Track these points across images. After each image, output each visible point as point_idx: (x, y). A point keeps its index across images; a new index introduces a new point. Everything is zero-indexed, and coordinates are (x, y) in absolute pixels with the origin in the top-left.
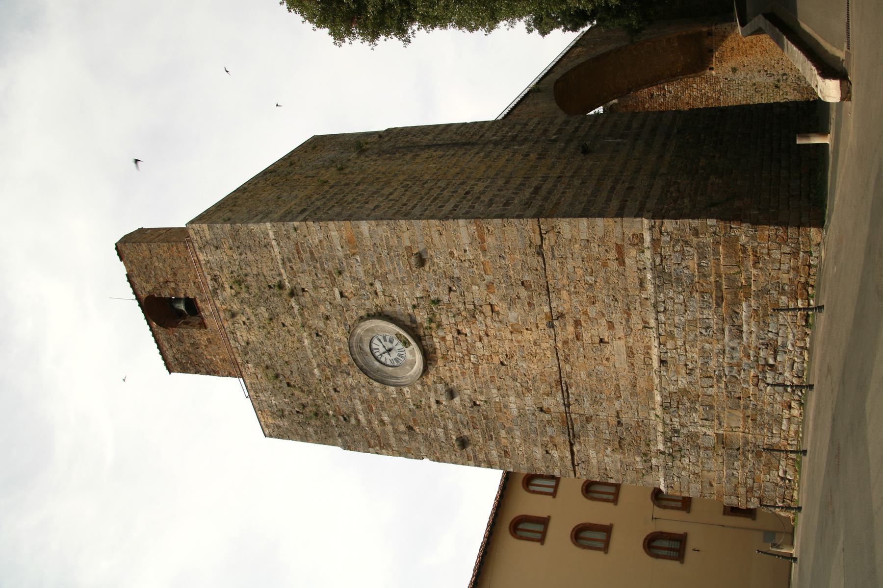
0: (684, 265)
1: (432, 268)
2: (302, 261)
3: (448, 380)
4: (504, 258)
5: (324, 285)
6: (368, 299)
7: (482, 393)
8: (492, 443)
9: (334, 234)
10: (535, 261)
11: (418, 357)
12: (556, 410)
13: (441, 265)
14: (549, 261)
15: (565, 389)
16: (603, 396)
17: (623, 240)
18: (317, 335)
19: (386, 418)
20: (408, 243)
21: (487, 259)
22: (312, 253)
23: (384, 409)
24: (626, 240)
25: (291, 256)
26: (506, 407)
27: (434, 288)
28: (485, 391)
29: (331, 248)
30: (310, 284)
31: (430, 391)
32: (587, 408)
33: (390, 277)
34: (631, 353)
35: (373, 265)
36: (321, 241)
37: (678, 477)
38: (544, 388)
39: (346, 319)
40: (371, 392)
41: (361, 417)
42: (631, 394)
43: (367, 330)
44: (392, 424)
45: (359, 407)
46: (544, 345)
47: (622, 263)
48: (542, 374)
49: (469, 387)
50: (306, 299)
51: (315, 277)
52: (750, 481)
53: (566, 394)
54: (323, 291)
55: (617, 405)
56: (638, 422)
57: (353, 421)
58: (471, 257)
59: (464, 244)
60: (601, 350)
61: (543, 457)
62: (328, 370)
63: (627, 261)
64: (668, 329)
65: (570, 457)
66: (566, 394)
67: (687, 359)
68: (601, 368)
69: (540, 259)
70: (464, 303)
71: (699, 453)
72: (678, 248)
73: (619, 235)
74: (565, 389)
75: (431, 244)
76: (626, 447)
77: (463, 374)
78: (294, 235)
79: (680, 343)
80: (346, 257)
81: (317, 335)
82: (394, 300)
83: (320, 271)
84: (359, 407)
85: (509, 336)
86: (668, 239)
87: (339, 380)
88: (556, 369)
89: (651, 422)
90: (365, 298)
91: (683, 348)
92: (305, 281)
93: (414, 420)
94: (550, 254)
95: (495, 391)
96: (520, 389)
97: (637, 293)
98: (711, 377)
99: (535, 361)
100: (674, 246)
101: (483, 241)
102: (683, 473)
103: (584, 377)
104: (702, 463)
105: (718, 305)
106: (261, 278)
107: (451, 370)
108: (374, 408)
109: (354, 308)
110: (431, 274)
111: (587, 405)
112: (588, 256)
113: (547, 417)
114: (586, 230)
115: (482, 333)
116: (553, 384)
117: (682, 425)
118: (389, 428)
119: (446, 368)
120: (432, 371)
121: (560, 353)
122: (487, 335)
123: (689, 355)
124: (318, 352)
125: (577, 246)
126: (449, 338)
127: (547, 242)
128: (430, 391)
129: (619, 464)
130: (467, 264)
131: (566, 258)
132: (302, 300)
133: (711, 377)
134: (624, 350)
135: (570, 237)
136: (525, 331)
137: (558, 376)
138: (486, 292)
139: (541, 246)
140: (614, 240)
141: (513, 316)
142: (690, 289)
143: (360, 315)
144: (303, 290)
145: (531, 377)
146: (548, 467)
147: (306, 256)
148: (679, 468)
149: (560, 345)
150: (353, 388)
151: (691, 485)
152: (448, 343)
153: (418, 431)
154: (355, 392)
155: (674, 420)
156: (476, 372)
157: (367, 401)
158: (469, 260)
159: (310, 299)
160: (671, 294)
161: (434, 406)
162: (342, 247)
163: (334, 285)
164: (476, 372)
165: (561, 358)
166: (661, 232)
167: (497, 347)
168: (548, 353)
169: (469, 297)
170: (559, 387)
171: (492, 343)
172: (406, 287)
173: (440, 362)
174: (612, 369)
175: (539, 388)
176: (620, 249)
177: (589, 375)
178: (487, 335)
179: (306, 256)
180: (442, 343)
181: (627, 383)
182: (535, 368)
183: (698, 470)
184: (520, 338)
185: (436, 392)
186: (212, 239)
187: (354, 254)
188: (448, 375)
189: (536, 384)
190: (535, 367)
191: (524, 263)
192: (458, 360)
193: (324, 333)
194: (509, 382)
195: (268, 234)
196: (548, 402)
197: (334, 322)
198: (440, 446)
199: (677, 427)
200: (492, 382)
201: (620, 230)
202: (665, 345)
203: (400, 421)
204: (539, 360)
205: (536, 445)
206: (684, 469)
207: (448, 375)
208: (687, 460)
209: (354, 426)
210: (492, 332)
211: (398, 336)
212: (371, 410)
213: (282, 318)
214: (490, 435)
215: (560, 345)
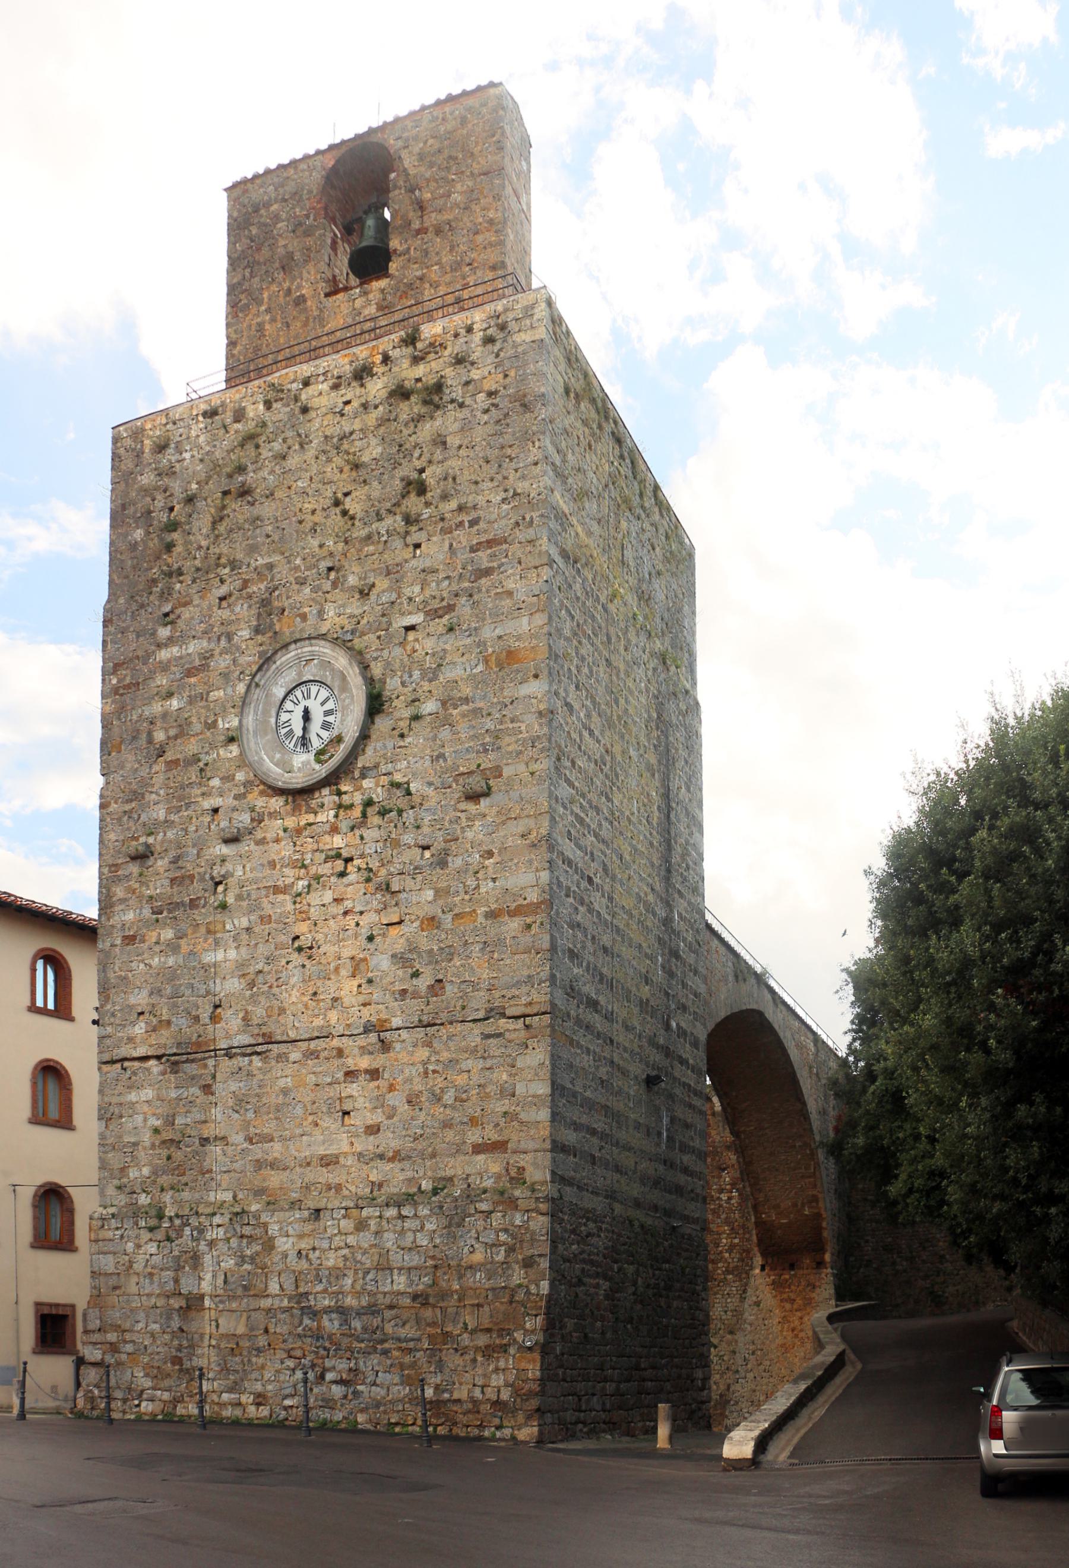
0: (476, 1246)
1: (463, 815)
2: (473, 550)
3: (259, 834)
4: (482, 950)
5: (428, 593)
6: (403, 684)
7: (239, 898)
8: (147, 912)
9: (524, 624)
10: (478, 1003)
11: (298, 780)
12: (220, 1034)
13: (469, 834)
14: (478, 1029)
15: (259, 1049)
16: (250, 1115)
17: (515, 1152)
18: (330, 569)
19: (175, 703)
20: (507, 772)
21: (481, 919)
22: (488, 572)
23: (191, 701)
24: (516, 1157)
25: (482, 525)
26: (217, 943)
27: (428, 818)
28: (245, 904)
29: (497, 617)
30: (428, 563)
31: (236, 797)
32: (227, 1088)
33: (445, 733)
34: (329, 1162)
35: (466, 700)
36: (510, 593)
37: (122, 1237)
38: (258, 1012)
39: (363, 634)
40: (225, 676)
41: (175, 651)
42: (258, 1161)
43: (344, 678)
44: (165, 715)
45: (193, 647)
46: (333, 1016)
47: (478, 1149)
48: (282, 1011)
49: (249, 875)
50: (399, 552)
51: (442, 575)
52: (129, 1348)
53: (250, 1051)
54: (417, 589)
55: (238, 1138)
56: (210, 1171)
57: (164, 632)
58: (483, 890)
59: (506, 878)
60: (329, 1113)
61: (131, 1007)
62: (262, 586)
63: (481, 1158)
64: (372, 1222)
65: (136, 1054)
66: (250, 1051)
67: (324, 1251)
68: (299, 1111)
69: (481, 1015)
70: (403, 873)
71: (168, 1269)
72: (503, 1237)
73: (523, 1145)
74: (259, 1049)
75: (506, 817)
76: (165, 1153)
77: (272, 864)
78: (521, 535)
79: (351, 1240)
80: (481, 644)
81: (330, 569)
82: (402, 736)
83: (455, 587)
84: (193, 647)
85: (346, 953)
86: (518, 1222)
87: (242, 609)
88: (293, 1035)
89: (212, 1194)
90: (406, 677)
91: (342, 1244)
92: (434, 551)
93: (176, 762)
94: (489, 1030)
95: (245, 923)
96: (251, 970)
97: (429, 1173)
98: (297, 1287)
99: (306, 999)
100: (506, 1230)
101: (513, 913)
102: (130, 1245)
103: (282, 1083)
104: (151, 1274)
105: (415, 1297)
106: (438, 455)
107: (277, 840)
108: (193, 680)
109: (385, 653)
110: (453, 814)
111: (233, 1086)
112: (488, 1095)
113: (205, 1017)
114: (531, 1092)
115: (348, 904)
116: (264, 1029)
117: (212, 1244)
118: (157, 708)
119: (281, 833)
120: (276, 803)
121: (320, 1044)
122: (346, 913)
123: (331, 1254)
124: (297, 568)
125: (505, 1077)
126: (338, 841)
127: (511, 1025)
128: (236, 797)
129: (133, 1140)
130: (471, 882)
131: (484, 1058)
132: (398, 543)
133: (297, 1287)
134: (332, 1150)
135: (519, 1064)
136: (356, 983)
137: (279, 1038)
138: (421, 914)
139: (503, 1015)
140: (514, 1137)
141: (382, 963)
142: (439, 1256)
143: (372, 664)
144: (417, 546)
145: (275, 990)
146: (113, 1015)
147: (483, 558)
148: (137, 1237)
149: (336, 1042)
150: (229, 637)
151: (110, 1257)
152: (327, 838)
153: (156, 768)
154: (223, 642)
155: (221, 1231)
156: (277, 890)
157: (204, 667)
158: (478, 887)
159: (398, 560)
160: (430, 1227)
161: (207, 804)
162: (500, 637)
163: (427, 613)
164: (277, 890)
165: (313, 1045)
166: (528, 1211)
167: (325, 930)
168: (319, 1022)
169: (409, 883)
170: (261, 1040)
171: (331, 922)
172: (428, 763)
173: (291, 822)
174: (298, 1131)
175: (256, 1003)
176: (499, 1146)
177: (285, 1092)
178: (346, 913)
179: (483, 558)
180: (327, 827)
181: (276, 1155)
182: (293, 997)
183: (138, 1267)
184: (344, 972)
185: (235, 809)
186: (515, 346)
187: (486, 661)
188: (270, 836)
189: (262, 999)
190: (294, 999)
191: (475, 986)
192: (298, 856)
193: (335, 585)
194: (263, 950)
195: (523, 477)
196: (232, 1020)
197: (355, 607)
198: (131, 811)
199: (210, 1235)
200: (262, 918)
201: (531, 1145)
202: (344, 1217)
203: (172, 732)
204: (306, 1006)
205: (151, 994)
206: (139, 1246)
207: (270, 836)
208: (154, 1250)
209: (154, 634)
210: (350, 921)
211: (339, 739)
212: (189, 673)
213: (360, 493)
214: (163, 910)
215: (336, 1042)
